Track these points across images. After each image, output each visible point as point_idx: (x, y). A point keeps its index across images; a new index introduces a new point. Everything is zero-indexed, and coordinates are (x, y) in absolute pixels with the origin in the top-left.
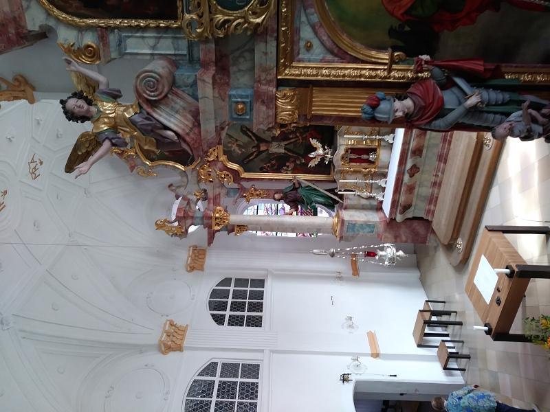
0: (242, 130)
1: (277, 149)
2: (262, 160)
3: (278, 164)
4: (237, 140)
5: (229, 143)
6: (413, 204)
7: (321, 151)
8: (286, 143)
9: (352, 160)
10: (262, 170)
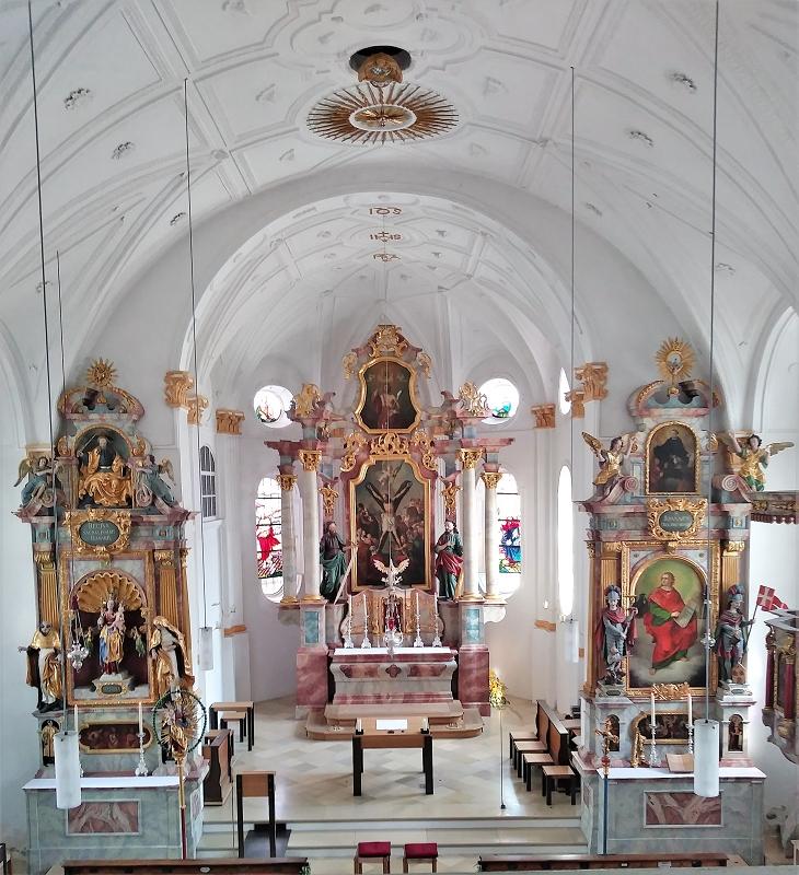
1: (387, 523)
2: (371, 505)
3: (368, 525)
5: (391, 468)
6: (352, 679)
7: (395, 571)
8: (395, 533)
10: (360, 506)
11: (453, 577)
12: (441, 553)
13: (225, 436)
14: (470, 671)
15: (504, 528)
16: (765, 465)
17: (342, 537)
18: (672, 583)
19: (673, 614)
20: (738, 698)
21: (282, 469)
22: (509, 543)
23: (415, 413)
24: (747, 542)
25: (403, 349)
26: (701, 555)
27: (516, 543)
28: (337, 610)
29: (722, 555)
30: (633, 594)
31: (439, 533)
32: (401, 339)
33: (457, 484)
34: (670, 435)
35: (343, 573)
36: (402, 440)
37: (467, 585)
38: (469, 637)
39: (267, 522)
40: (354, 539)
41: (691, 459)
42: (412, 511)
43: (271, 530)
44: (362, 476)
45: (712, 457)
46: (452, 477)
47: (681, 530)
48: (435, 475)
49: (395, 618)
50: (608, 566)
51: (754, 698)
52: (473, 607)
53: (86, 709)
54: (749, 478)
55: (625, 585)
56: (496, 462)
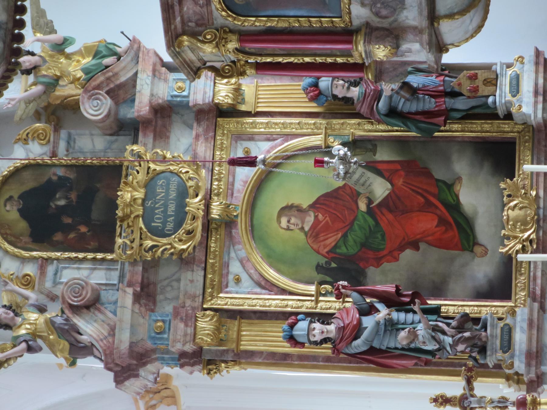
16: (66, 42)
18: (299, 209)
19: (363, 206)
29: (248, 114)
30: (312, 289)
41: (61, 172)
45: (63, 134)
47: (183, 193)
55: (290, 303)
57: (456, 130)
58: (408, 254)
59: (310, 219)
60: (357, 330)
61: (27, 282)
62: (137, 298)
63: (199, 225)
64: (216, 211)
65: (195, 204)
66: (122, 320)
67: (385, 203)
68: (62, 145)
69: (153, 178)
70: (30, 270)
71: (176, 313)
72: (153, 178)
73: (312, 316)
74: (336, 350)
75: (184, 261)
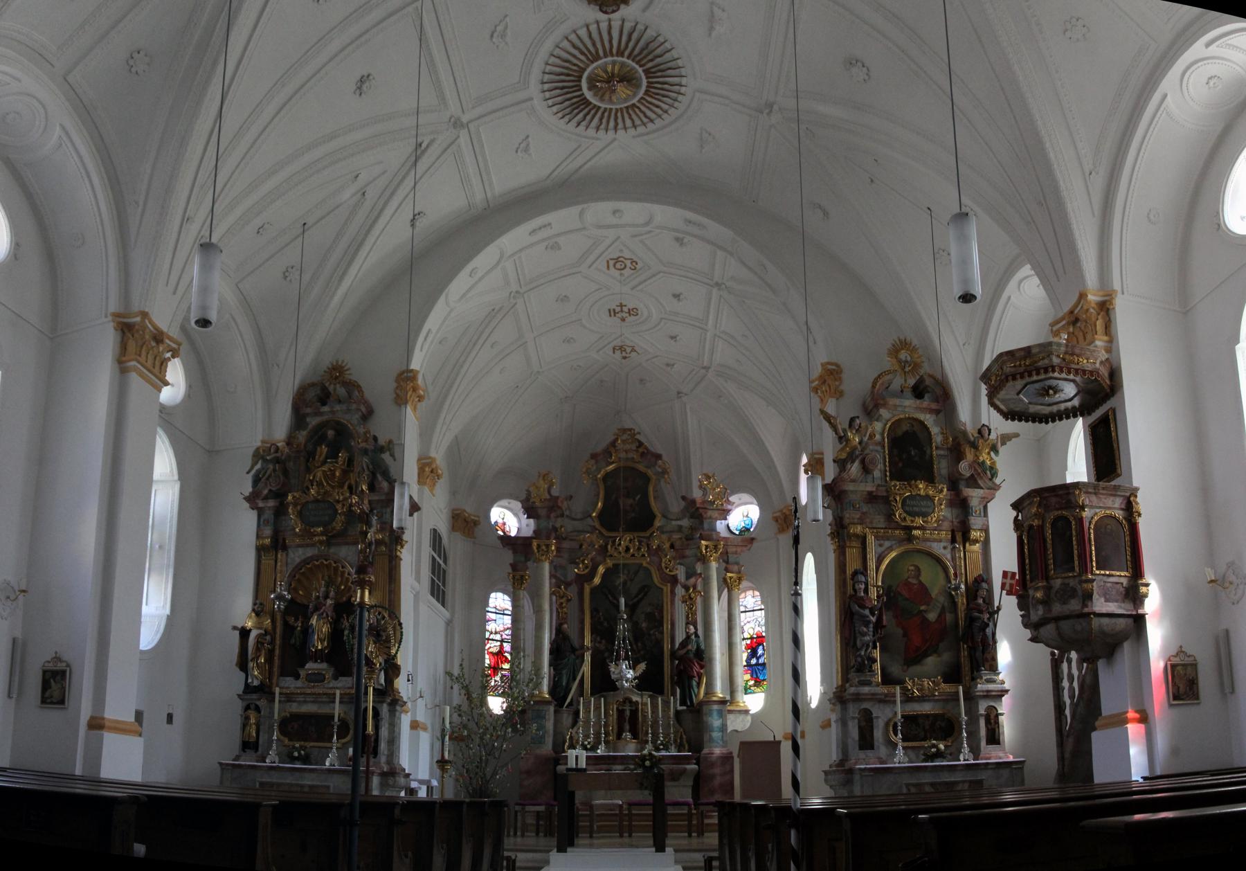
0: (644, 587)
4: (632, 580)
9: (621, 713)
10: (594, 611)
11: (694, 683)
12: (681, 659)
13: (458, 535)
14: (713, 777)
15: (748, 647)
16: (997, 452)
17: (574, 636)
19: (923, 608)
20: (991, 687)
21: (514, 567)
22: (754, 661)
23: (653, 517)
24: (986, 530)
25: (643, 454)
26: (945, 548)
27: (761, 661)
28: (567, 719)
31: (680, 637)
32: (641, 444)
33: (699, 588)
34: (905, 427)
35: (574, 679)
36: (640, 542)
37: (710, 686)
38: (711, 739)
39: (498, 637)
40: (587, 642)
41: (928, 452)
42: (650, 617)
43: (501, 646)
44: (597, 580)
46: (692, 580)
47: (924, 515)
48: (674, 580)
49: (630, 721)
50: (852, 553)
51: (1007, 686)
52: (715, 707)
53: (288, 698)
54: (984, 462)
55: (872, 572)
56: (737, 563)
57: (964, 653)
58: (900, 631)
59: (914, 581)
60: (863, 607)
61: (872, 436)
62: (870, 493)
63: (909, 523)
64: (916, 533)
65: (920, 521)
66: (858, 487)
67: (925, 620)
68: (942, 452)
69: (931, 499)
70: (878, 437)
71: (863, 513)
72: (931, 499)
73: (866, 584)
74: (851, 596)
75: (890, 516)
